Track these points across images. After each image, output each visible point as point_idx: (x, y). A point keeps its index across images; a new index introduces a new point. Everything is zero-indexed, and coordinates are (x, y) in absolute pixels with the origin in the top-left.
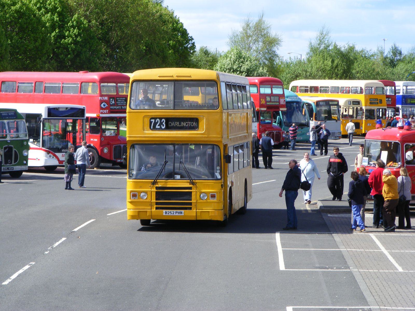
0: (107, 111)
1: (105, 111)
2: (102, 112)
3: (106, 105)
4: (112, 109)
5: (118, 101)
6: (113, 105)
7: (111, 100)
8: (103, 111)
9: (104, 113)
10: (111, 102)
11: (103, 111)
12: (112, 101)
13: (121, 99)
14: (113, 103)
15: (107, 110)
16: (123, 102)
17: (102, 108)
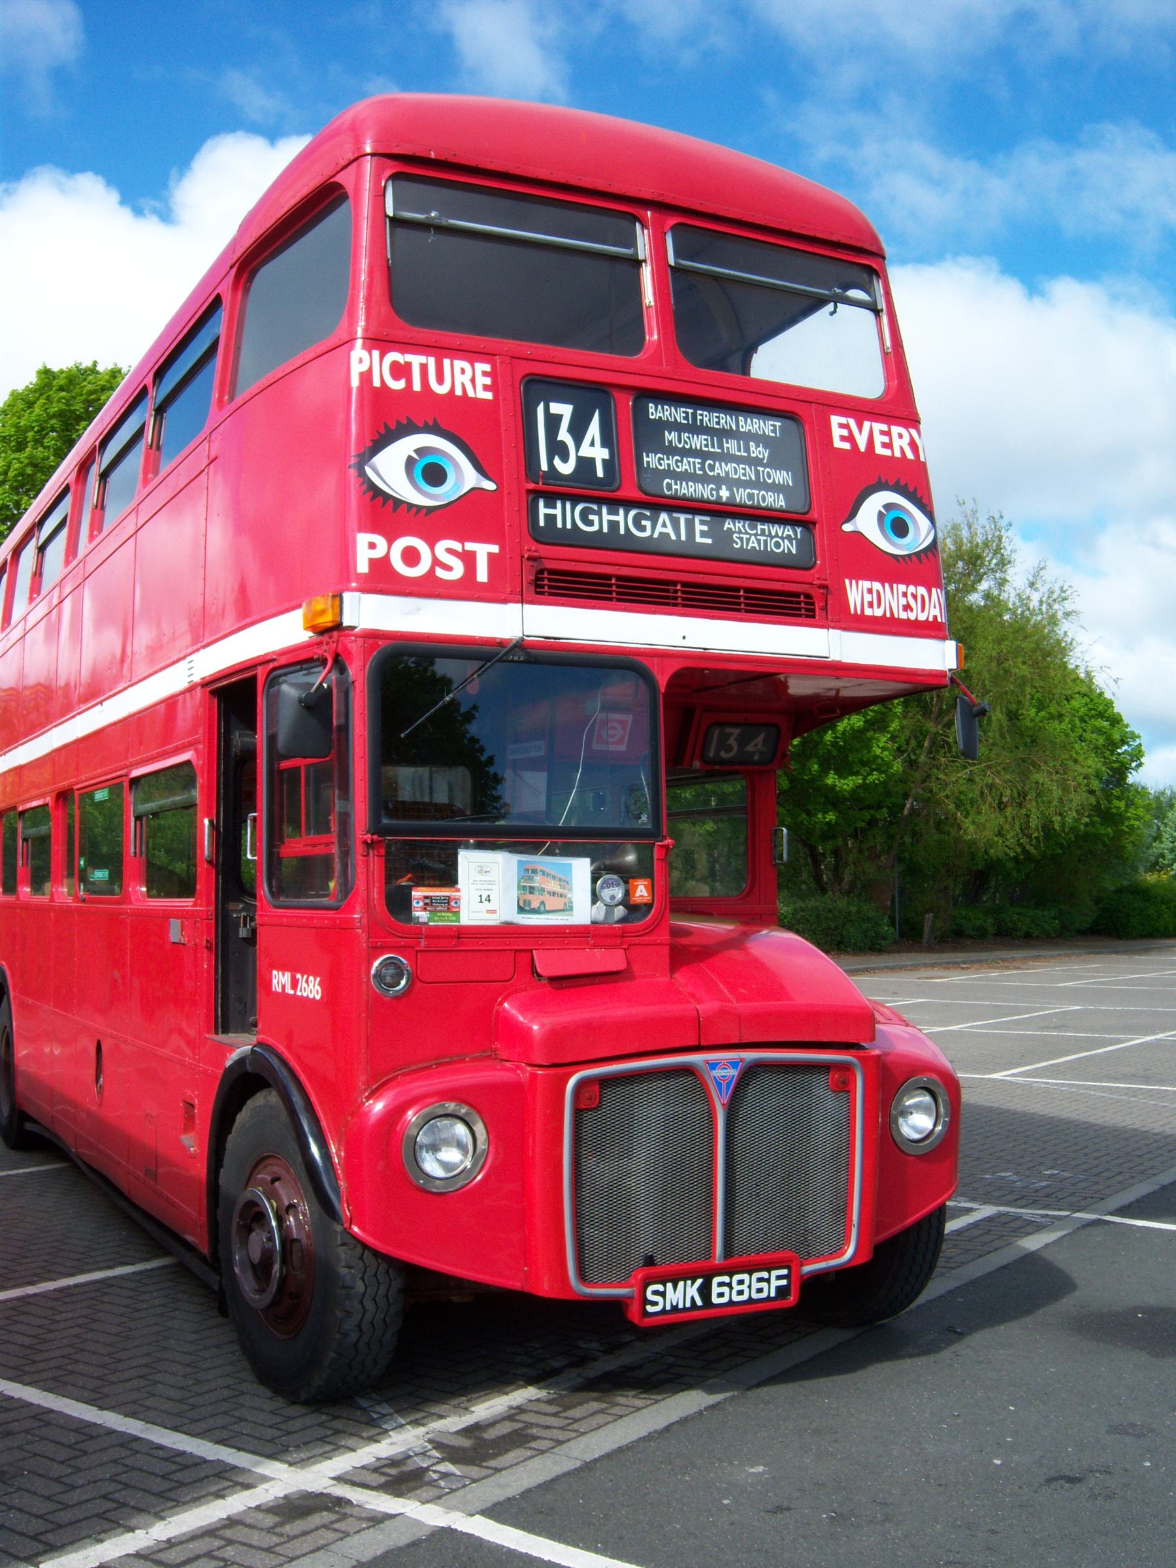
0: (469, 559)
1: (444, 556)
2: (381, 566)
3: (465, 477)
4: (573, 538)
5: (671, 451)
6: (584, 488)
7: (553, 422)
8: (411, 556)
9: (429, 588)
10: (558, 449)
11: (411, 556)
12: (564, 435)
13: (707, 418)
14: (586, 464)
16: (744, 472)
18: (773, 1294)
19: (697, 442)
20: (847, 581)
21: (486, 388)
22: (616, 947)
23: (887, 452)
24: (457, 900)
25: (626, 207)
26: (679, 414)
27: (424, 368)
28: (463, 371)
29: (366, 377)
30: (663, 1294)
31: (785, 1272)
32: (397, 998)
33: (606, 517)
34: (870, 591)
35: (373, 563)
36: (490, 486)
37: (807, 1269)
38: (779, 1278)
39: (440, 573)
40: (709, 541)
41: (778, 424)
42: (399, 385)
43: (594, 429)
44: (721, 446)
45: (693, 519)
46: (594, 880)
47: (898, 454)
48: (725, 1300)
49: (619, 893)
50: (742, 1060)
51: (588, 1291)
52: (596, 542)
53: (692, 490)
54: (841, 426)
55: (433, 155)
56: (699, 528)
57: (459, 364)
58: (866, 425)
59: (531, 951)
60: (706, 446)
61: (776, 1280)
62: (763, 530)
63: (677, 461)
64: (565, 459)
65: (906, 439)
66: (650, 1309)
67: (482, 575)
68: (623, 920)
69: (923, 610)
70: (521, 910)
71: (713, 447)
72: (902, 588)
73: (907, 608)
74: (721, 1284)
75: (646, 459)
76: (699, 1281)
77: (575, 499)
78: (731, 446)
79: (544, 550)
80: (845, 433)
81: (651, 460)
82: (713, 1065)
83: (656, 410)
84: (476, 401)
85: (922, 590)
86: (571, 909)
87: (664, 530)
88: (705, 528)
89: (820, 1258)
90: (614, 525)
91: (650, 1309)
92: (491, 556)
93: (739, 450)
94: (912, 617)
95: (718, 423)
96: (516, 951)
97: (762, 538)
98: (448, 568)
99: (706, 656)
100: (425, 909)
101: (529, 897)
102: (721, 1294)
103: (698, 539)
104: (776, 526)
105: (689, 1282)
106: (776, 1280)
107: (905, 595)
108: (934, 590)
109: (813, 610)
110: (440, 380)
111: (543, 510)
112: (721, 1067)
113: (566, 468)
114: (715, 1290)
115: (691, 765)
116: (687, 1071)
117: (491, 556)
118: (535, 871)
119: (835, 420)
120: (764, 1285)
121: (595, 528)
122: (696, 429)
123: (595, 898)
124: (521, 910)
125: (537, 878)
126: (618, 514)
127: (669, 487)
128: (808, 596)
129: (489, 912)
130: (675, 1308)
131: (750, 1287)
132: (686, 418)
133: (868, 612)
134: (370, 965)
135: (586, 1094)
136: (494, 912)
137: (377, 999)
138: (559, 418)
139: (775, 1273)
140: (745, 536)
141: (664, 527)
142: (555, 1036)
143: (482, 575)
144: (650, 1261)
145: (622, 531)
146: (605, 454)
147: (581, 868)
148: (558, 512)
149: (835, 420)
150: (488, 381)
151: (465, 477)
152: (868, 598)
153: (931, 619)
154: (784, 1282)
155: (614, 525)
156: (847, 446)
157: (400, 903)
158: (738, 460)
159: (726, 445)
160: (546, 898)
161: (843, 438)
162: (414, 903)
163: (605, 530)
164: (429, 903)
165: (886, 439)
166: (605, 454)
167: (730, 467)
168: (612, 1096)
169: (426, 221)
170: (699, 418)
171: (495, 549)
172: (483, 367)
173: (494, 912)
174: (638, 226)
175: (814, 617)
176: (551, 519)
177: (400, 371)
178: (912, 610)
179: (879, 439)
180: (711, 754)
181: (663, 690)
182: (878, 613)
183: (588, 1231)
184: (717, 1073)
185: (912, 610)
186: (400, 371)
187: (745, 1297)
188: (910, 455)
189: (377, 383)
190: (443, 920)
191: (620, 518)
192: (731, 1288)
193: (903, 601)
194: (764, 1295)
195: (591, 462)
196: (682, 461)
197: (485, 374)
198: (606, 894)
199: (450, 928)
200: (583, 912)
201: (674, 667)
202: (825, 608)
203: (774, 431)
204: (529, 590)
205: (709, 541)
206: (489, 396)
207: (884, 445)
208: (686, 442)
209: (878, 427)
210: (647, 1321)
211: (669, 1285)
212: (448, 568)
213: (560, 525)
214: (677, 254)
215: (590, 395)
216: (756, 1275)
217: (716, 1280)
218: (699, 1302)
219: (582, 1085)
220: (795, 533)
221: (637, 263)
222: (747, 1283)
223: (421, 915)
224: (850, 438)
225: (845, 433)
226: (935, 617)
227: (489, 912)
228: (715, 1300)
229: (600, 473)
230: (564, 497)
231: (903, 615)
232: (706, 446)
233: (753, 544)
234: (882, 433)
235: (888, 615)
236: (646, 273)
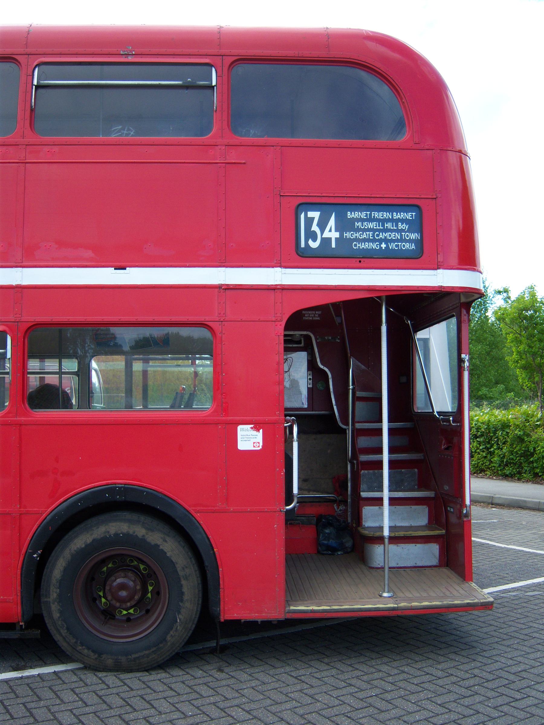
5: (358, 230)
19: (371, 225)
44: (383, 226)
63: (361, 234)
78: (389, 225)
83: (351, 214)
93: (393, 227)
132: (366, 216)
158: (392, 231)
159: (386, 225)
170: (373, 215)
196: (363, 234)
203: (412, 217)
208: (365, 226)
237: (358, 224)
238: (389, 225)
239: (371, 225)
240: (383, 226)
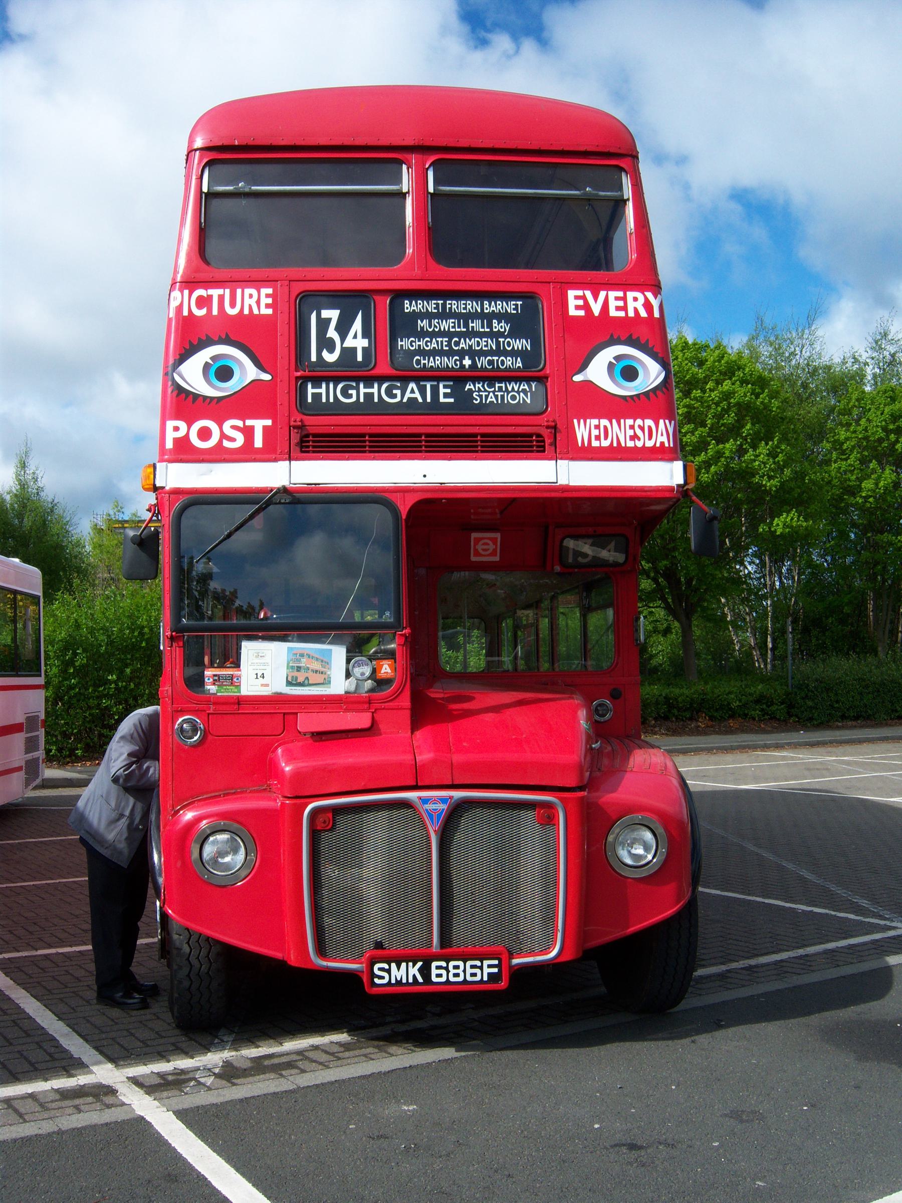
0: (248, 432)
3: (247, 372)
5: (422, 334)
6: (349, 371)
7: (323, 324)
8: (205, 434)
9: (219, 455)
10: (326, 344)
11: (205, 434)
12: (332, 333)
13: (454, 305)
15: (259, 425)
17: (183, 404)
18: (485, 978)
19: (446, 325)
20: (575, 421)
21: (267, 306)
22: (363, 711)
23: (622, 314)
24: (239, 677)
25: (384, 156)
26: (431, 306)
27: (221, 298)
28: (251, 296)
29: (180, 308)
30: (389, 971)
31: (496, 962)
32: (195, 746)
33: (362, 390)
34: (597, 427)
35: (176, 441)
36: (267, 377)
37: (515, 961)
38: (489, 966)
39: (226, 444)
40: (452, 400)
41: (519, 303)
42: (202, 312)
43: (357, 325)
44: (466, 325)
45: (438, 386)
46: (348, 661)
47: (631, 314)
48: (443, 979)
49: (367, 670)
50: (451, 798)
51: (325, 963)
52: (355, 409)
53: (438, 362)
54: (577, 298)
55: (236, 143)
56: (442, 390)
57: (248, 291)
58: (602, 294)
59: (296, 714)
60: (453, 327)
61: (488, 968)
62: (500, 389)
63: (427, 342)
64: (331, 350)
65: (641, 300)
66: (377, 981)
67: (258, 443)
68: (372, 690)
69: (650, 438)
70: (289, 683)
71: (459, 327)
72: (630, 422)
73: (634, 437)
74: (438, 968)
75: (400, 343)
76: (420, 964)
77: (336, 380)
78: (476, 325)
79: (310, 420)
80: (581, 302)
81: (404, 343)
82: (425, 801)
84: (260, 316)
85: (649, 422)
86: (329, 682)
87: (413, 396)
88: (449, 391)
89: (531, 953)
90: (368, 396)
91: (377, 981)
92: (265, 428)
94: (639, 444)
95: (465, 308)
96: (284, 714)
97: (499, 394)
98: (233, 440)
99: (442, 488)
100: (214, 684)
101: (296, 674)
102: (439, 973)
103: (442, 400)
104: (513, 384)
105: (411, 964)
106: (488, 968)
107: (632, 427)
108: (661, 422)
109: (544, 446)
110: (233, 305)
111: (310, 390)
112: (433, 802)
113: (330, 357)
114: (434, 972)
115: (553, 569)
116: (405, 804)
117: (265, 428)
118: (302, 655)
119: (571, 294)
120: (478, 971)
121: (354, 399)
122: (444, 315)
123: (348, 675)
124: (289, 683)
125: (304, 660)
126: (321, 388)
127: (418, 362)
128: (539, 435)
129: (262, 685)
130: (399, 983)
131: (464, 971)
132: (437, 308)
133: (595, 444)
134: (173, 723)
135: (320, 819)
136: (267, 685)
137: (180, 748)
138: (329, 320)
139: (486, 963)
140: (484, 394)
141: (412, 391)
142: (297, 776)
143: (258, 443)
144: (379, 945)
145: (376, 400)
146: (365, 343)
147: (339, 653)
148: (323, 390)
149: (571, 294)
150: (270, 301)
151: (247, 372)
152: (595, 432)
153: (658, 445)
154: (495, 970)
155: (368, 396)
156: (581, 313)
157: (197, 682)
158: (481, 335)
159: (471, 325)
160: (309, 674)
161: (578, 308)
162: (206, 680)
163: (362, 400)
164: (217, 680)
165: (621, 303)
166: (365, 343)
167: (473, 342)
168: (344, 822)
169: (236, 191)
170: (448, 306)
171: (269, 422)
172: (265, 291)
173: (267, 685)
174: (404, 167)
175: (544, 451)
176: (316, 396)
177: (203, 302)
178: (639, 439)
179: (613, 304)
180: (570, 560)
181: (404, 517)
182: (605, 443)
183: (327, 921)
184: (428, 807)
185: (639, 439)
186: (203, 302)
187: (461, 979)
188: (643, 314)
189: (185, 313)
190: (228, 692)
191: (375, 390)
192: (448, 972)
193: (630, 433)
194: (478, 978)
195: (354, 350)
197: (267, 296)
198: (357, 671)
199: (232, 697)
200: (339, 685)
201: (411, 500)
202: (554, 444)
204: (295, 450)
205: (452, 400)
206: (270, 311)
207: (618, 309)
208: (435, 326)
209: (612, 294)
210: (375, 990)
211: (393, 965)
212: (233, 440)
213: (324, 400)
214: (436, 182)
215: (350, 301)
216: (469, 963)
217: (434, 964)
218: (420, 980)
219: (315, 812)
220: (530, 387)
221: (403, 195)
222: (462, 968)
223: (212, 689)
224: (586, 307)
225: (580, 302)
226: (662, 443)
227: (262, 685)
228: (434, 979)
229: (360, 358)
230: (328, 379)
231: (630, 444)
232: (453, 327)
233: (491, 398)
234: (617, 299)
235: (615, 445)
236: (409, 202)
237: (423, 324)
238: (476, 325)
239: (446, 325)
240: (466, 325)
